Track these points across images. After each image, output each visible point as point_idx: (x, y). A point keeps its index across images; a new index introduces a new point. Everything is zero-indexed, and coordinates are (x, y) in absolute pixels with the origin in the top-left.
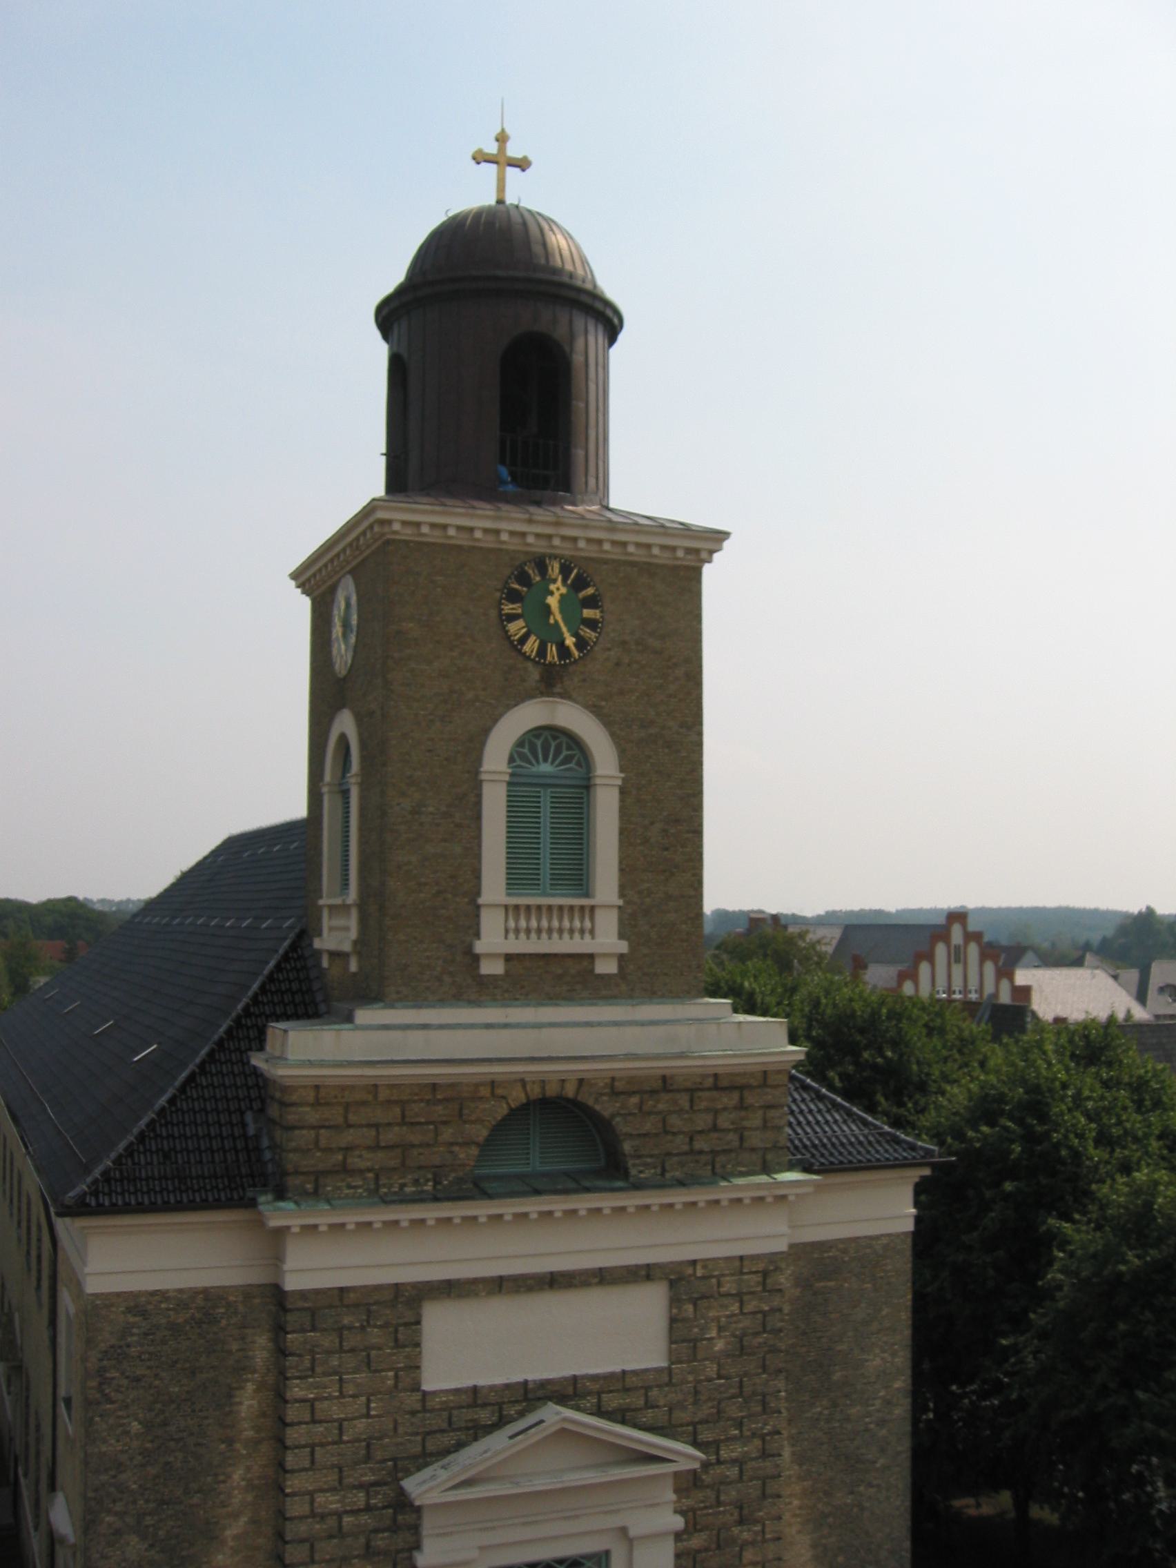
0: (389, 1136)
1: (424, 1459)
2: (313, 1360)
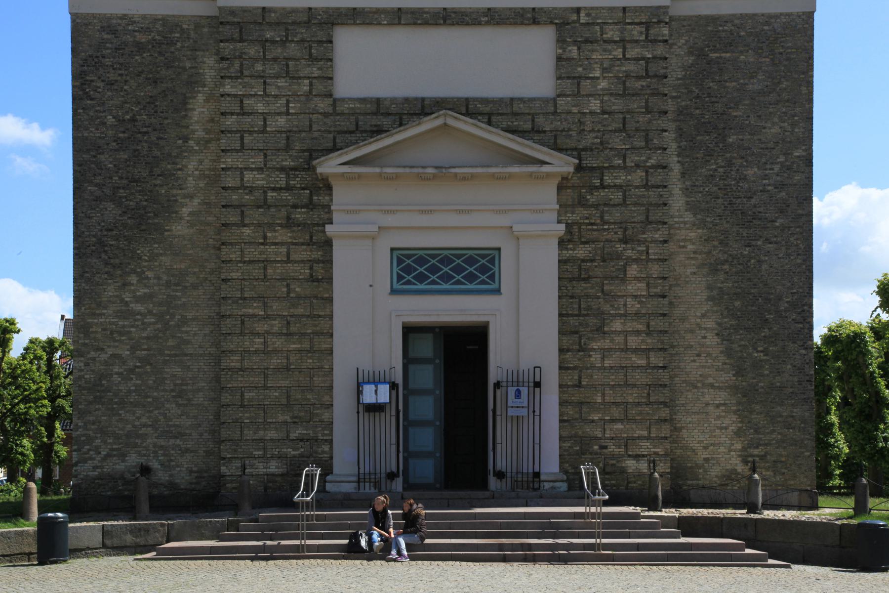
2: (242, 65)
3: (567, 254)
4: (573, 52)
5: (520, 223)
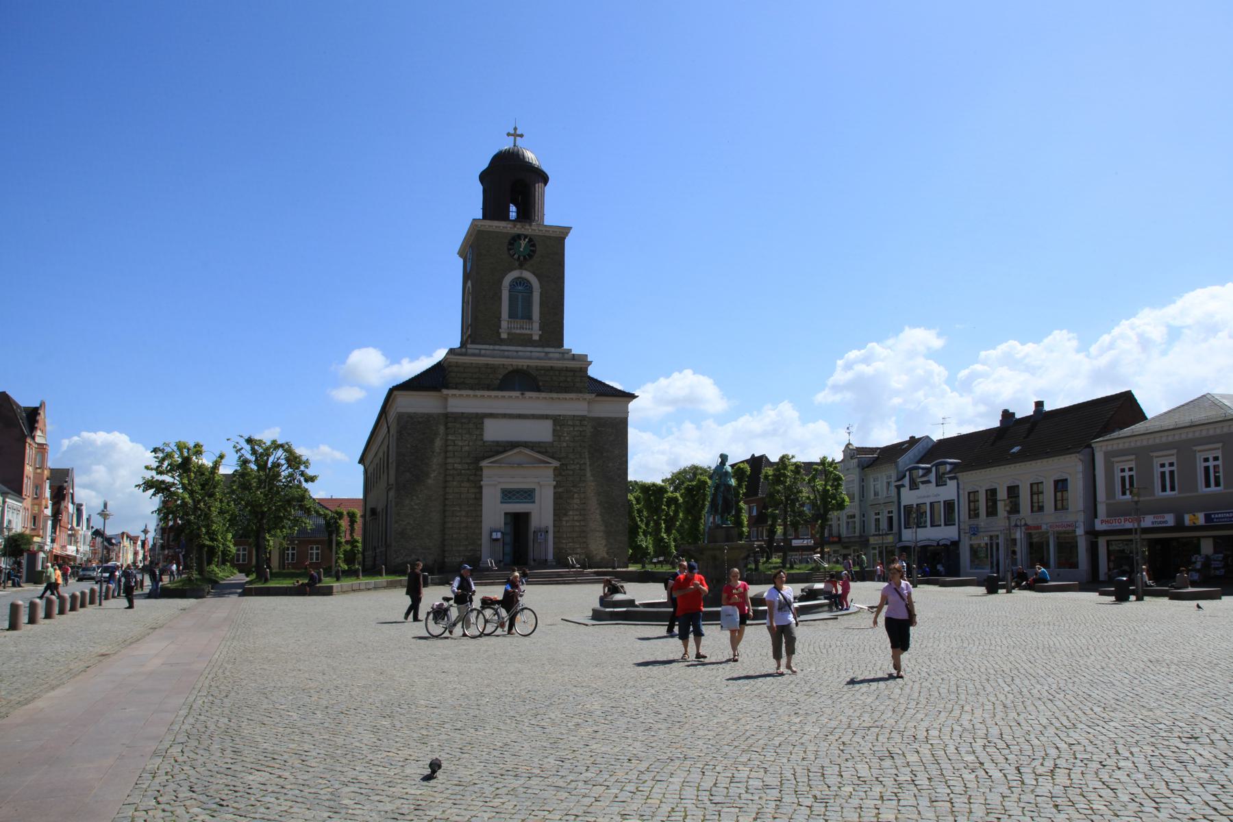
1: (484, 458)
5: (542, 482)
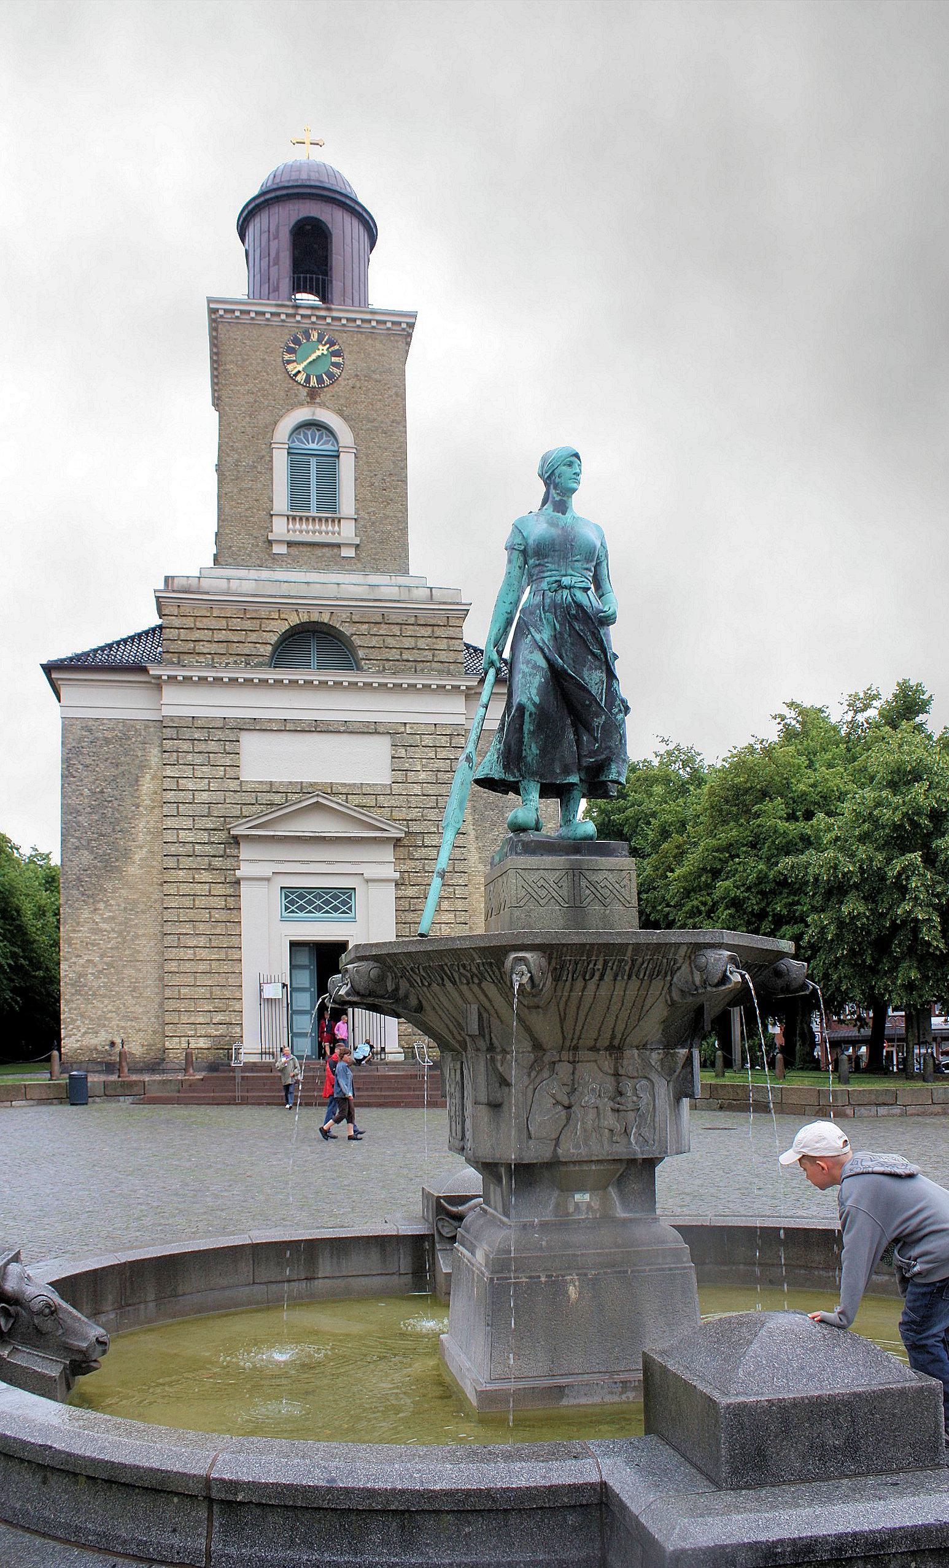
0: (222, 635)
3: (401, 893)
4: (402, 752)
